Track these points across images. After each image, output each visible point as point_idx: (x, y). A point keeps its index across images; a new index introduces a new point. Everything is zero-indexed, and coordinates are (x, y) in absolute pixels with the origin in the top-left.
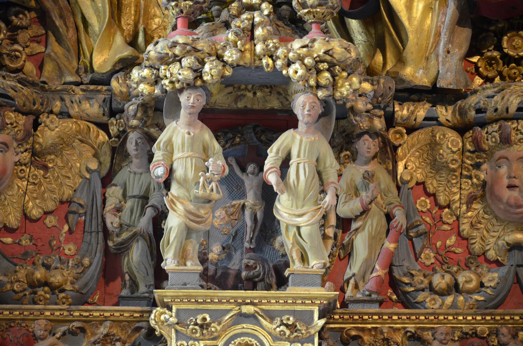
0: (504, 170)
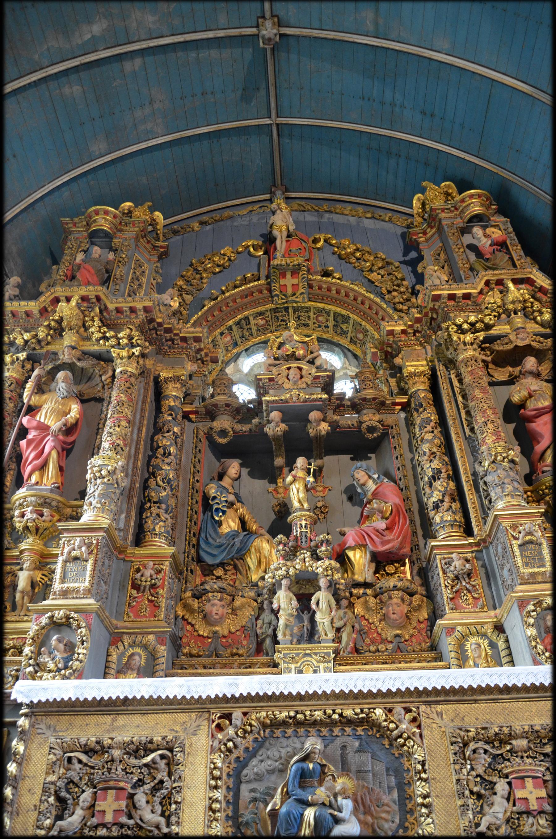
0: (390, 608)
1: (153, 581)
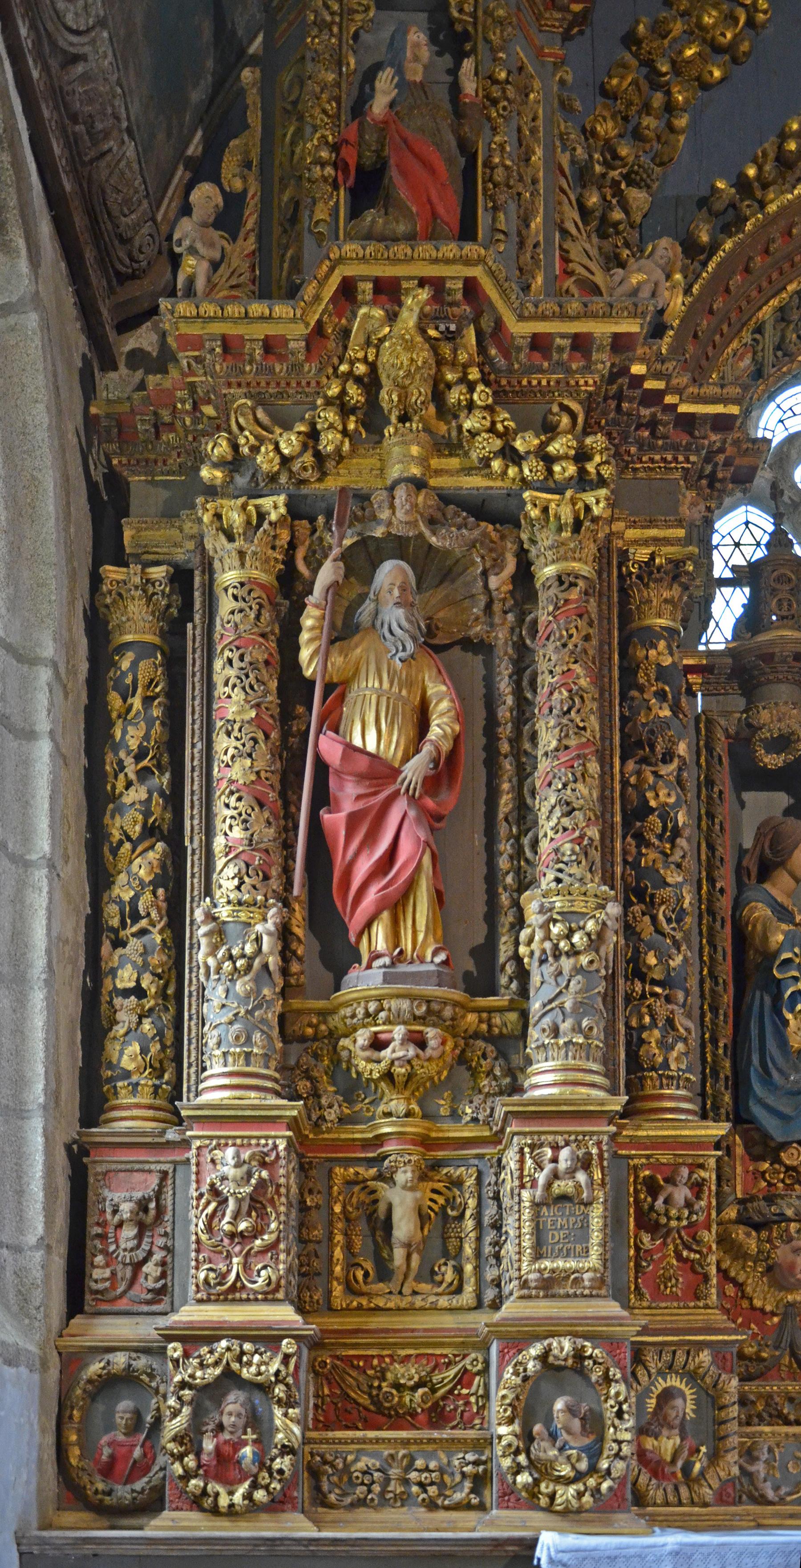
1: (695, 1217)
